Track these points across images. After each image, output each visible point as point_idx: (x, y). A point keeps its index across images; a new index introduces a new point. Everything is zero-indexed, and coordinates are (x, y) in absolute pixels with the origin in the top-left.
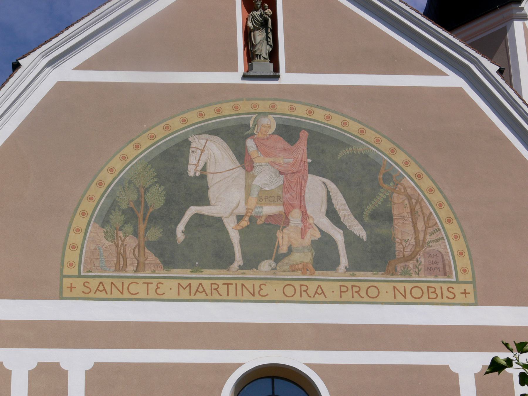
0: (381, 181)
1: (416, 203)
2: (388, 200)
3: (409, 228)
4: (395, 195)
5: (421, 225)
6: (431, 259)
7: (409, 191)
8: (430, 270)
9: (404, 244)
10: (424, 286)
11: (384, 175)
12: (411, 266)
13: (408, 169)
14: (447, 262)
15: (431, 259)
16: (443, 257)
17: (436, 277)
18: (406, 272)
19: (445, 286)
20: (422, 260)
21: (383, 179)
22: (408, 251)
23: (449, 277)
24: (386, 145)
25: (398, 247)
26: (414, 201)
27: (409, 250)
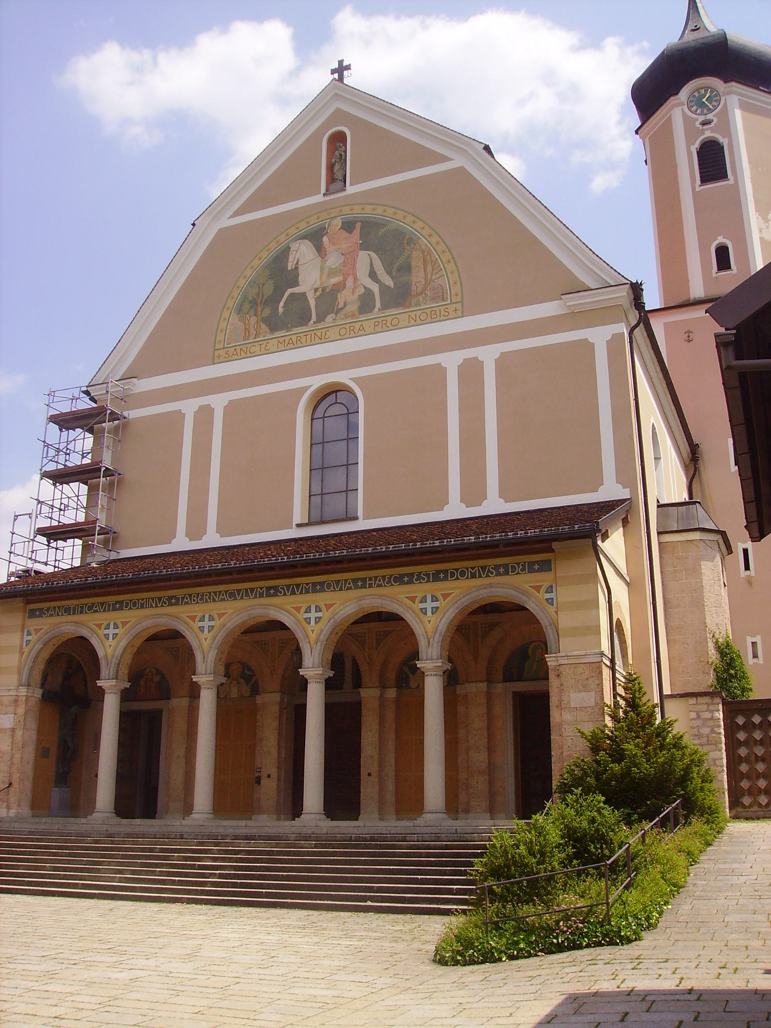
0: (406, 245)
1: (427, 254)
2: (409, 257)
3: (422, 274)
4: (413, 252)
5: (429, 269)
6: (435, 292)
7: (423, 247)
8: (433, 299)
9: (418, 285)
10: (428, 311)
11: (407, 240)
12: (421, 299)
13: (423, 232)
14: (445, 291)
15: (435, 292)
16: (442, 289)
17: (437, 303)
18: (418, 304)
19: (442, 308)
20: (429, 293)
21: (407, 243)
22: (419, 290)
23: (446, 301)
24: (410, 219)
25: (414, 287)
26: (426, 253)
27: (420, 288)
